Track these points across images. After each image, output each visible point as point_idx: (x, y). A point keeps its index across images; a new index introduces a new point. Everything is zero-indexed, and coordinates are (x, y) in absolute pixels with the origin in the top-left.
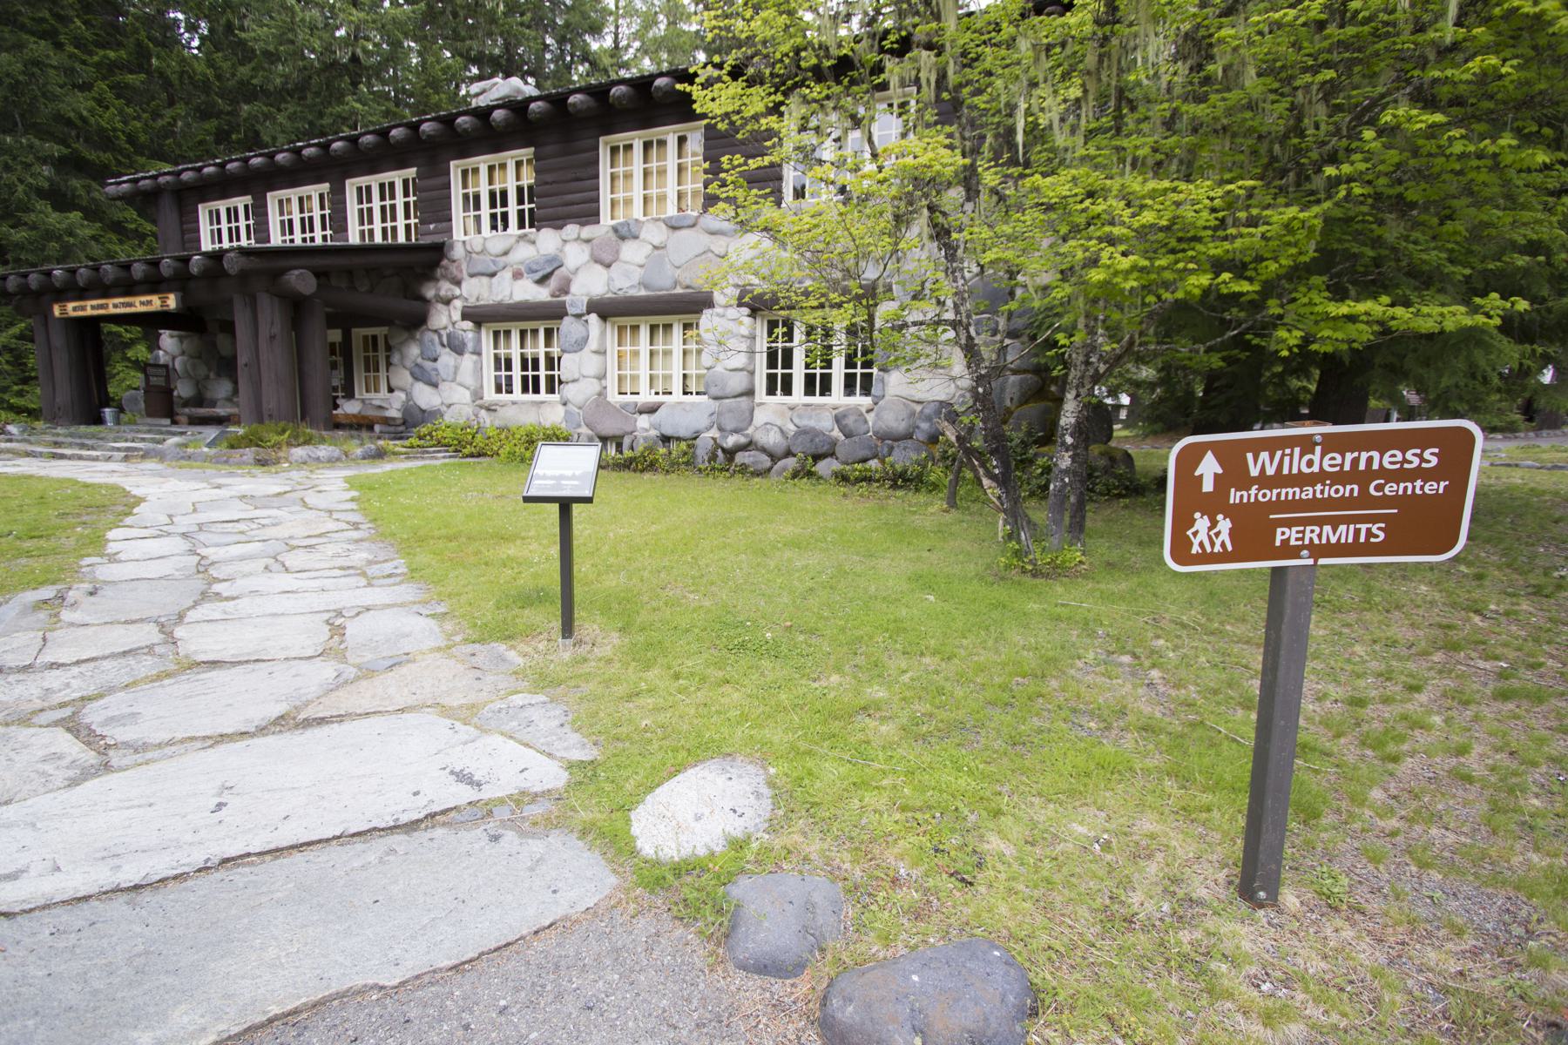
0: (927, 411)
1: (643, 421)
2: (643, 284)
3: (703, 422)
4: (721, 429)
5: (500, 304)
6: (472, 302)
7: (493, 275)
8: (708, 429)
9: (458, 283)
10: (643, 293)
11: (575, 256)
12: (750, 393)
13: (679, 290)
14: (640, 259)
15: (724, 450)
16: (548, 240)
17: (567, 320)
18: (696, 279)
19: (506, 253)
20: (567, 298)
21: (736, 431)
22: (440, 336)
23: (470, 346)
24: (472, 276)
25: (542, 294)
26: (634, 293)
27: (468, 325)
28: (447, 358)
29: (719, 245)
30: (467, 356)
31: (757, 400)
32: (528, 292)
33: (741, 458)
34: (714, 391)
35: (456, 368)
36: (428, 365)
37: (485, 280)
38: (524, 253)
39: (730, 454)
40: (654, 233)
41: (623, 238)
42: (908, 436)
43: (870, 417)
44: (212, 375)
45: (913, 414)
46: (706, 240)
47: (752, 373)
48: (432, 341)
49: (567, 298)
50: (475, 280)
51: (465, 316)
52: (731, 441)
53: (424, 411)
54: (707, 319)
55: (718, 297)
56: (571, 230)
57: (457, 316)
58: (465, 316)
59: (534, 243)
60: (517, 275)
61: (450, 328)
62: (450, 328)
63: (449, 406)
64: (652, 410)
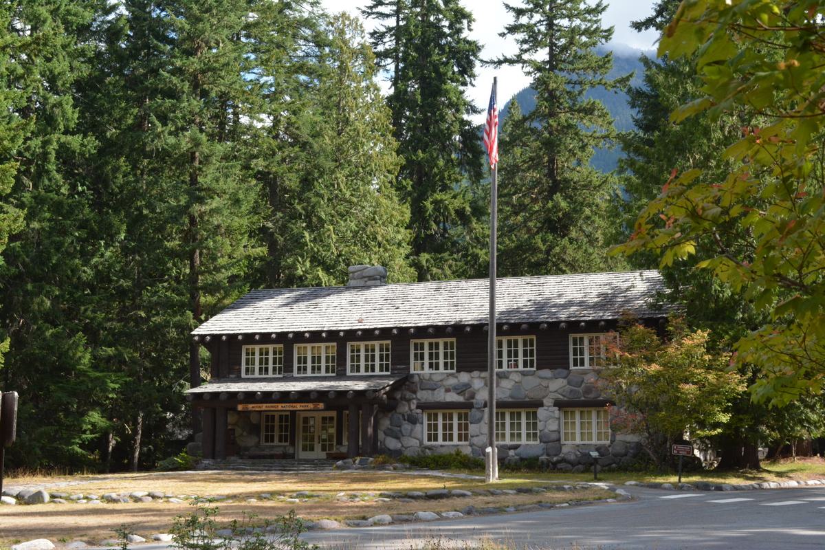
0: (632, 446)
1: (512, 453)
2: (511, 397)
3: (541, 452)
4: (548, 455)
5: (438, 402)
6: (423, 401)
7: (435, 389)
8: (542, 455)
9: (415, 392)
10: (510, 400)
11: (478, 384)
12: (559, 440)
13: (527, 399)
14: (510, 387)
15: (552, 463)
16: (464, 377)
17: (473, 410)
18: (535, 395)
19: (441, 381)
20: (474, 401)
21: (556, 455)
22: (403, 416)
23: (420, 420)
24: (422, 390)
25: (461, 399)
26: (506, 400)
27: (419, 411)
28: (407, 426)
29: (544, 383)
30: (418, 425)
31: (562, 443)
32: (453, 397)
33: (559, 466)
34: (544, 440)
35: (412, 430)
36: (396, 429)
37: (430, 392)
38: (452, 381)
39: (555, 464)
40: (516, 377)
41: (501, 378)
42: (626, 455)
43: (610, 449)
44: (245, 434)
45: (626, 447)
46: (538, 381)
47: (559, 432)
48: (399, 418)
49: (474, 401)
50: (424, 392)
51: (418, 407)
52: (555, 459)
53: (389, 450)
54: (541, 412)
55: (545, 401)
56: (476, 373)
57: (413, 407)
58: (418, 407)
59: (456, 377)
60: (448, 390)
61: (409, 412)
62: (409, 412)
63: (406, 448)
64: (515, 447)
